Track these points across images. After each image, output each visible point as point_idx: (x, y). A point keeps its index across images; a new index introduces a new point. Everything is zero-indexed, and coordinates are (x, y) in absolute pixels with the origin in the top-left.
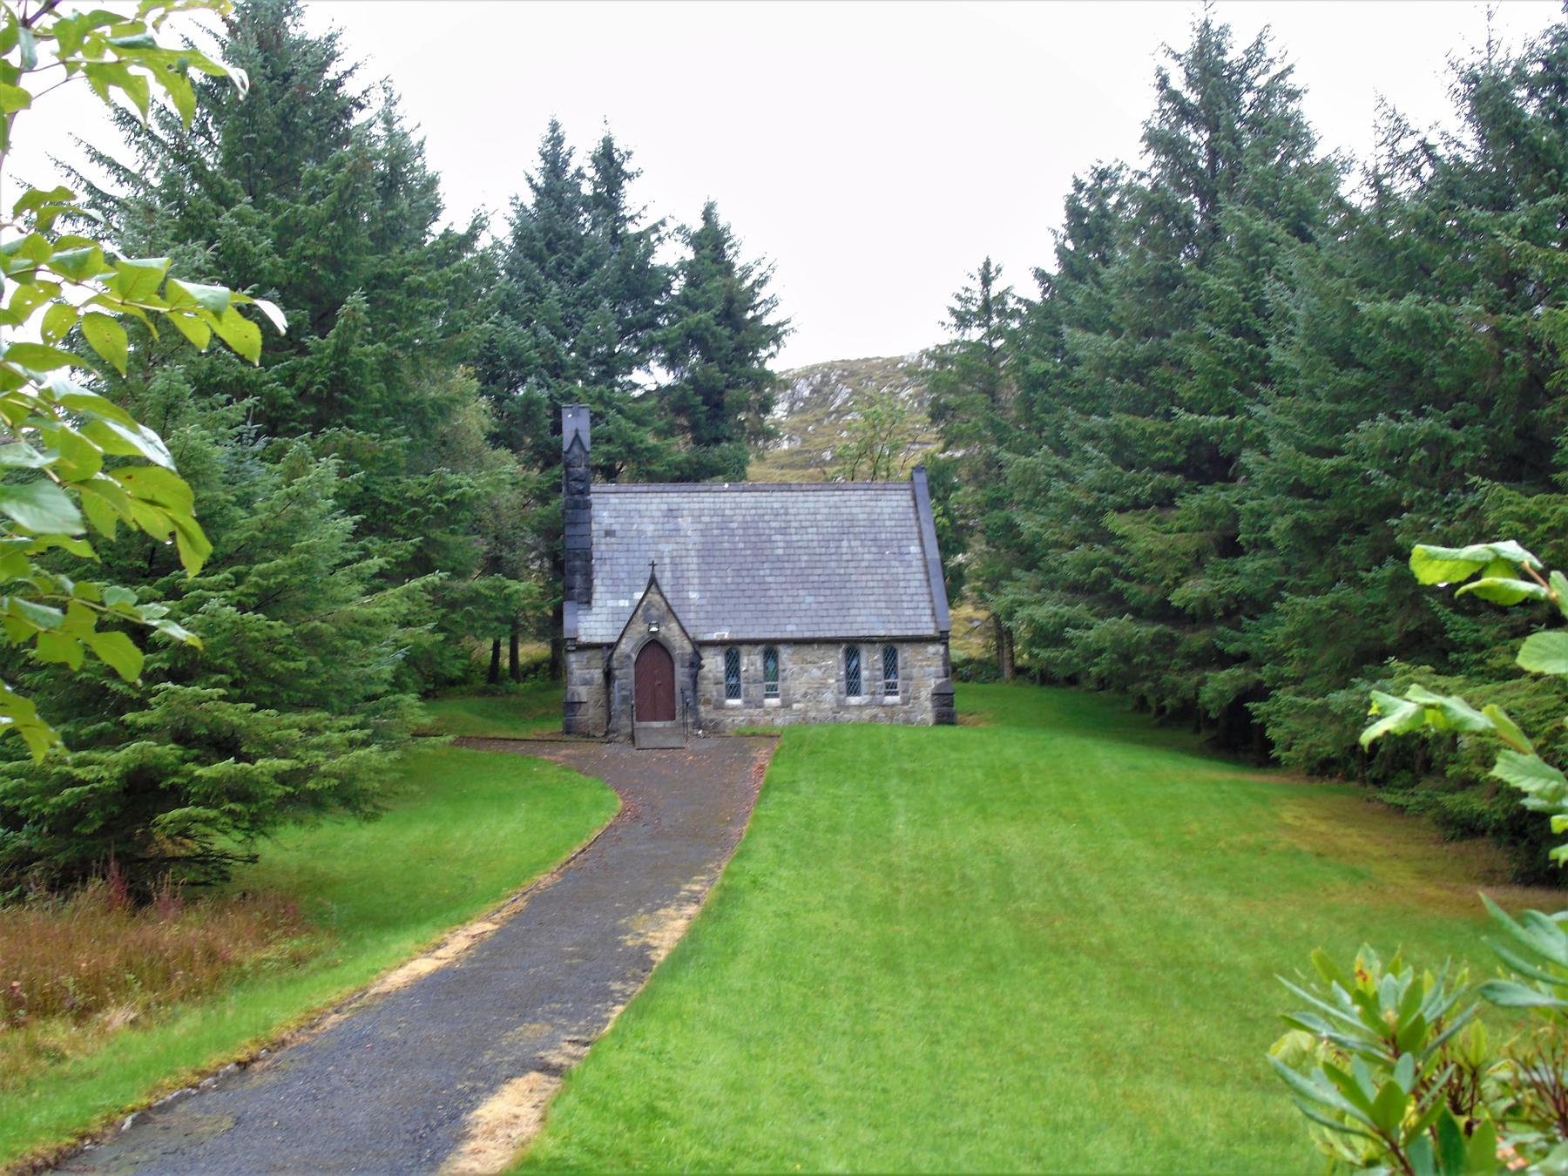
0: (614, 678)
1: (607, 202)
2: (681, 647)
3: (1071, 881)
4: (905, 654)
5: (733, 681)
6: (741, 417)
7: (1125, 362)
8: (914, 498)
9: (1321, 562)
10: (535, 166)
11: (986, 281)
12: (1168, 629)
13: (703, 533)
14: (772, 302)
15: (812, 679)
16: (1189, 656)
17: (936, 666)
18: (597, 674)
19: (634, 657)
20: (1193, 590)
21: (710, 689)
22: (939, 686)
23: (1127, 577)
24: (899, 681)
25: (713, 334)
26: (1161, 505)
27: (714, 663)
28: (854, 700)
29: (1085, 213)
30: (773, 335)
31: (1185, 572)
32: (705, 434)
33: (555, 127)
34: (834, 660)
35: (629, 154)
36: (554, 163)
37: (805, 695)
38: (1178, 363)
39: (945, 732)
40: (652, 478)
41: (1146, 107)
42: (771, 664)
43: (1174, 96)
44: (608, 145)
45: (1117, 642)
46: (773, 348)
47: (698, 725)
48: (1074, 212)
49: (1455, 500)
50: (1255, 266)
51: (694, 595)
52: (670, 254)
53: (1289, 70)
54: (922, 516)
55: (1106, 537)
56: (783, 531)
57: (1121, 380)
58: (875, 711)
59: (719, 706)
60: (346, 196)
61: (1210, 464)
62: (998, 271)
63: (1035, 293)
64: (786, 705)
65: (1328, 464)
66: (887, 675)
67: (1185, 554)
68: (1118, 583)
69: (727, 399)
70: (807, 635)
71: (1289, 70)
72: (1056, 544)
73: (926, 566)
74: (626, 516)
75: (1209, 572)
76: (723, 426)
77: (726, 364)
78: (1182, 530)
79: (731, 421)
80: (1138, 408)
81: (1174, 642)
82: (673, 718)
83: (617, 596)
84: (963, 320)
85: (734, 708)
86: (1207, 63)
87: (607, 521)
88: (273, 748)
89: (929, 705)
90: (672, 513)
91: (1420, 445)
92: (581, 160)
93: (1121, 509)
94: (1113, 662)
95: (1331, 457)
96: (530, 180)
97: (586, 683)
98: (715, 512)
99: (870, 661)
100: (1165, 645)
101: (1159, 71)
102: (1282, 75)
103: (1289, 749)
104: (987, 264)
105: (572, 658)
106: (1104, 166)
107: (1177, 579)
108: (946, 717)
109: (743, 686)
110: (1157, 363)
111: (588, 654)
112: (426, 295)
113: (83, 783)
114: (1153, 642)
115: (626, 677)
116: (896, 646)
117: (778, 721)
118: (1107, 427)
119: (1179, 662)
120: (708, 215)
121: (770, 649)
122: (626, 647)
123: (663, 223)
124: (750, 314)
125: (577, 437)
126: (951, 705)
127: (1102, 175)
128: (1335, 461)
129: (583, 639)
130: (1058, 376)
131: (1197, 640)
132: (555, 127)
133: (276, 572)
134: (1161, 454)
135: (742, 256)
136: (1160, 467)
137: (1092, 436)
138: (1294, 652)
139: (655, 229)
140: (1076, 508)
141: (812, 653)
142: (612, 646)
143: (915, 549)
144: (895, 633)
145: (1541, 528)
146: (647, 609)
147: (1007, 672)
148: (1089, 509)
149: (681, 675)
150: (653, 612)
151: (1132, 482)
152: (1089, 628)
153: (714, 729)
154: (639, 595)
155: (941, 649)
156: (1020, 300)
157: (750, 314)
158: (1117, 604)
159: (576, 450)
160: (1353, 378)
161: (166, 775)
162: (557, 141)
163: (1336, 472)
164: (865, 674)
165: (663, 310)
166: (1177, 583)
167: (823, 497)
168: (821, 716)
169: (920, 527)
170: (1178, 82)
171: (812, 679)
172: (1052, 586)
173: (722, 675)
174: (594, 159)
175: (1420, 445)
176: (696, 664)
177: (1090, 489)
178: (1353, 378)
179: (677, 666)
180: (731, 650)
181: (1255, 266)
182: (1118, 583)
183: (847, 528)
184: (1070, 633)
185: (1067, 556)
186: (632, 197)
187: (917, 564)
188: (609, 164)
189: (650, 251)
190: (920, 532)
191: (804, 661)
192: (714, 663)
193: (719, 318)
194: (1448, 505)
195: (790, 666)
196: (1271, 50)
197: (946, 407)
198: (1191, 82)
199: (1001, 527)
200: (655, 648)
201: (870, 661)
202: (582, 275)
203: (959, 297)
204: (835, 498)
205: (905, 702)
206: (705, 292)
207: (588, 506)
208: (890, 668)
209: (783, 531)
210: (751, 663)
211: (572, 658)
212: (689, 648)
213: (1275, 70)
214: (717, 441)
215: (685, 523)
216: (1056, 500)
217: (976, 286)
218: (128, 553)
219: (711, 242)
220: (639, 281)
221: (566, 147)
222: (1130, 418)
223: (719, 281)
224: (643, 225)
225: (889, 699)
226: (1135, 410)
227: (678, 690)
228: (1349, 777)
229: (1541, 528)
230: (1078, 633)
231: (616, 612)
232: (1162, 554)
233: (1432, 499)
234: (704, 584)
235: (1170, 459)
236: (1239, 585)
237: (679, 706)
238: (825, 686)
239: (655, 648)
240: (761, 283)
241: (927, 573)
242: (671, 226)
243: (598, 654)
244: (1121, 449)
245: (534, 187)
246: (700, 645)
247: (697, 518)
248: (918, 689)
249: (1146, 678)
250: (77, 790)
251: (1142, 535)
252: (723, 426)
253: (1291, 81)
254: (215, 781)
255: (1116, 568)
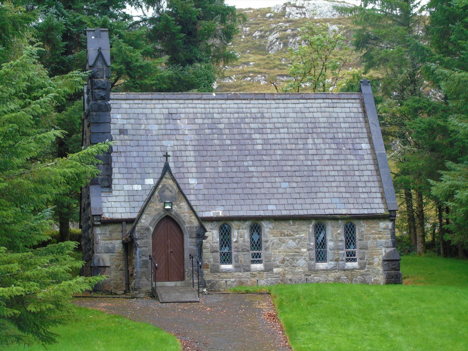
2: (189, 222)
4: (362, 228)
5: (226, 250)
8: (363, 106)
13: (198, 132)
15: (288, 247)
17: (386, 239)
18: (118, 244)
19: (152, 229)
21: (209, 257)
22: (388, 254)
24: (357, 250)
27: (213, 235)
28: (321, 265)
34: (306, 232)
37: (283, 261)
39: (392, 289)
47: (202, 284)
54: (370, 120)
58: (338, 274)
59: (216, 270)
64: (268, 269)
66: (348, 245)
69: (200, 28)
70: (284, 213)
73: (375, 159)
74: (135, 116)
76: (195, 50)
79: (202, 46)
82: (182, 278)
85: (227, 272)
87: (120, 122)
89: (380, 269)
90: (171, 116)
97: (109, 251)
98: (206, 115)
99: (334, 235)
105: (98, 231)
108: (394, 278)
109: (234, 254)
116: (355, 222)
117: (262, 282)
121: (255, 224)
122: (145, 221)
125: (100, 55)
129: (107, 216)
141: (287, 227)
142: (130, 221)
143: (365, 146)
144: (354, 212)
147: (420, 247)
149: (189, 244)
150: (167, 193)
153: (213, 288)
154: (150, 182)
155: (390, 224)
159: (99, 64)
164: (330, 244)
167: (291, 104)
168: (295, 278)
169: (368, 128)
171: (288, 247)
173: (217, 245)
176: (201, 235)
180: (225, 224)
183: (312, 128)
187: (368, 158)
190: (369, 133)
191: (282, 234)
192: (213, 235)
195: (271, 238)
199: (425, 130)
200: (169, 221)
204: (300, 105)
207: (108, 109)
208: (350, 240)
209: (260, 131)
210: (240, 235)
212: (196, 223)
214: (191, 62)
215: (183, 124)
225: (350, 265)
227: (186, 256)
231: (132, 195)
234: (201, 171)
237: (188, 268)
238: (300, 254)
243: (119, 228)
246: (203, 220)
247: (192, 121)
252: (195, 50)
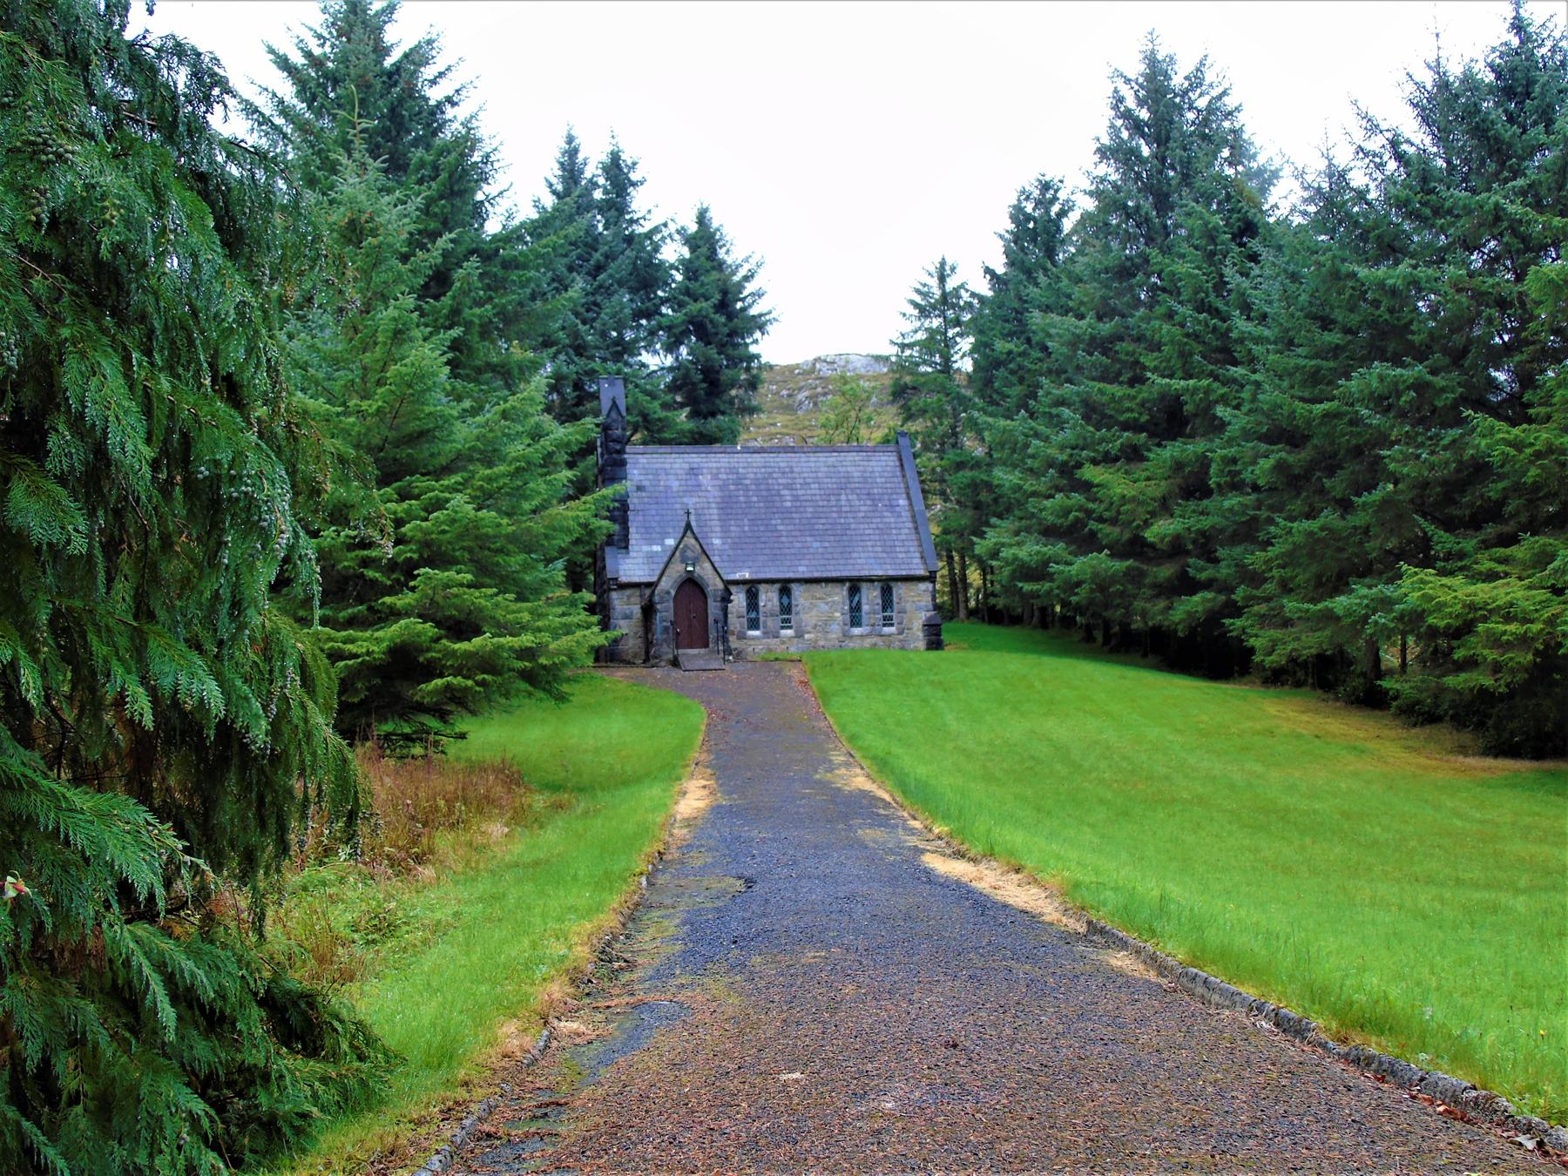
0: (655, 611)
1: (616, 206)
2: (714, 584)
3: (1125, 758)
4: (900, 590)
5: (753, 615)
6: (733, 392)
7: (1093, 338)
8: (901, 460)
9: (1299, 494)
10: (553, 172)
11: (942, 279)
12: (1137, 564)
13: (723, 487)
14: (758, 295)
15: (821, 610)
16: (1155, 586)
17: (926, 600)
18: (636, 610)
19: (673, 593)
20: (1161, 530)
21: (735, 623)
22: (929, 619)
23: (1101, 520)
24: (894, 614)
25: (711, 321)
26: (1129, 460)
27: (739, 599)
28: (856, 631)
29: (1029, 218)
30: (759, 323)
31: (1153, 514)
32: (703, 407)
33: (570, 139)
34: (839, 595)
35: (634, 164)
36: (571, 169)
37: (815, 627)
38: (1139, 339)
39: (933, 654)
40: (662, 442)
41: (1099, 124)
42: (785, 601)
43: (1127, 115)
44: (615, 158)
45: (1095, 575)
46: (757, 335)
47: (728, 651)
48: (1018, 216)
49: (1437, 435)
50: (1213, 254)
51: (717, 542)
52: (672, 252)
53: (1224, 93)
54: (908, 474)
55: (1086, 487)
56: (790, 487)
57: (1091, 354)
58: (874, 640)
59: (742, 637)
60: (457, 176)
61: (1171, 420)
62: (953, 269)
63: (984, 288)
64: (799, 635)
65: (1319, 408)
66: (884, 609)
67: (1153, 499)
68: (1093, 525)
69: (723, 378)
70: (816, 575)
71: (1224, 93)
72: (1034, 494)
73: (913, 516)
75: (1178, 512)
76: (718, 401)
77: (722, 348)
78: (1148, 479)
79: (726, 397)
80: (1106, 377)
81: (1142, 574)
82: (707, 646)
83: (651, 542)
84: (924, 312)
85: (754, 638)
86: (1155, 83)
87: (637, 478)
88: (503, 628)
89: (921, 634)
90: (693, 472)
91: (1408, 388)
92: (592, 169)
93: (1095, 462)
94: (1092, 591)
95: (1321, 402)
96: (551, 185)
97: (626, 617)
98: (732, 470)
99: (870, 597)
100: (1134, 577)
101: (1116, 91)
102: (1220, 97)
103: (1270, 654)
104: (943, 264)
105: (614, 595)
106: (1047, 178)
107: (1146, 522)
108: (935, 641)
109: (762, 619)
110: (1121, 339)
111: (628, 592)
112: (517, 268)
113: (356, 656)
114: (1125, 574)
115: (665, 612)
116: (892, 584)
117: (792, 650)
118: (1078, 394)
119: (1148, 592)
120: (702, 219)
121: (785, 587)
122: (668, 584)
123: (665, 225)
124: (739, 305)
125: (614, 405)
126: (938, 634)
127: (1046, 186)
128: (1326, 406)
129: (623, 579)
130: (1020, 355)
131: (1165, 572)
132: (570, 139)
133: (498, 477)
134: (1129, 415)
135: (732, 254)
136: (1126, 426)
137: (1061, 402)
138: (1275, 572)
139: (656, 230)
140: (1051, 464)
141: (819, 590)
142: (650, 585)
143: (903, 502)
144: (891, 573)
145: (1528, 451)
146: (684, 551)
147: (962, 613)
148: (1064, 464)
149: (713, 608)
150: (689, 554)
151: (1102, 440)
152: (1071, 564)
153: (739, 655)
154: (671, 542)
155: (930, 586)
156: (973, 295)
157: (739, 305)
158: (1089, 543)
159: (614, 415)
160: (1334, 338)
161: (422, 651)
162: (572, 153)
163: (1327, 415)
164: (865, 608)
165: (664, 301)
166: (1147, 524)
167: (822, 457)
168: (827, 644)
170: (1131, 103)
171: (821, 610)
172: (1028, 530)
173: (744, 610)
174: (604, 169)
175: (1408, 388)
176: (726, 599)
177: (1062, 448)
178: (1334, 338)
179: (710, 601)
180: (752, 588)
181: (1213, 254)
182: (1093, 525)
183: (845, 484)
184: (1054, 567)
185: (1048, 503)
186: (639, 202)
187: (906, 515)
188: (618, 174)
189: (656, 249)
190: (907, 488)
191: (814, 597)
192: (739, 599)
193: (713, 310)
194: (1430, 438)
195: (802, 601)
196: (1209, 77)
197: (906, 387)
198: (1141, 103)
199: (968, 486)
200: (691, 586)
201: (870, 597)
202: (599, 268)
203: (918, 291)
204: (832, 459)
205: (901, 632)
206: (703, 285)
207: (623, 463)
208: (887, 603)
209: (790, 487)
210: (769, 598)
211: (614, 595)
212: (721, 586)
213: (1215, 93)
214: (713, 414)
215: (705, 479)
216: (1033, 457)
217: (934, 282)
218: (1189, 214)
219: (704, 241)
220: (647, 276)
221: (580, 157)
222: (1101, 385)
223: (715, 275)
224: (646, 227)
225: (887, 630)
226: (1103, 378)
227: (711, 620)
228: (1298, 684)
229: (1528, 451)
230: (1061, 567)
231: (651, 556)
232: (1133, 499)
233: (1418, 434)
234: (725, 532)
235: (1135, 420)
236: (1206, 523)
237: (712, 635)
238: (832, 619)
239: (691, 586)
240: (747, 278)
241: (915, 522)
242: (672, 227)
243: (637, 592)
244: (1092, 412)
245: (554, 192)
246: (728, 583)
247: (715, 477)
248: (910, 620)
249: (1118, 605)
250: (350, 662)
251: (1115, 483)
252: (718, 401)
253: (1229, 102)
254: (469, 655)
255: (1089, 513)
